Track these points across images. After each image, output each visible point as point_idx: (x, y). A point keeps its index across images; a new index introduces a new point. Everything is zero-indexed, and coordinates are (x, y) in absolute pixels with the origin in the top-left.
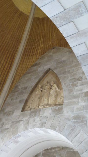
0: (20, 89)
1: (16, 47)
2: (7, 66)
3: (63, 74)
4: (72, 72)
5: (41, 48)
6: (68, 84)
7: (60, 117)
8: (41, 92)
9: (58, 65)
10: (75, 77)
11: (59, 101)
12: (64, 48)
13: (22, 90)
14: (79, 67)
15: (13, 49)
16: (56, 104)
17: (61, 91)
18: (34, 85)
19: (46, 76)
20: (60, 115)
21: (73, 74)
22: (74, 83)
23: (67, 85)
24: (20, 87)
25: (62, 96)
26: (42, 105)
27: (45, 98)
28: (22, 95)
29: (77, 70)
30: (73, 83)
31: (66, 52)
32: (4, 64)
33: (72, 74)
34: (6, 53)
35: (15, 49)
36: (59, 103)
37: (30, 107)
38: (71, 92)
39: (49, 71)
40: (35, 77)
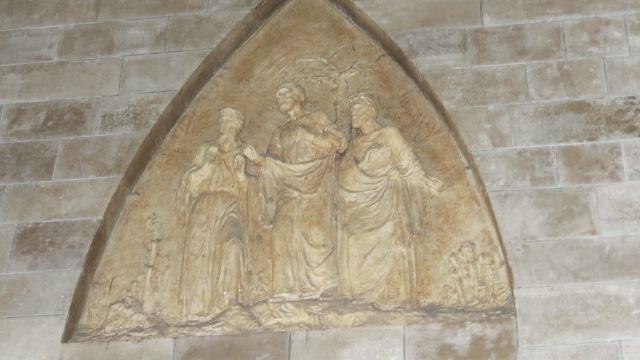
3: (463, 47)
4: (545, 54)
6: (525, 144)
8: (241, 176)
10: (582, 97)
14: (606, 15)
21: (560, 67)
22: (586, 143)
23: (520, 153)
27: (306, 236)
28: (43, 183)
29: (594, 43)
30: (574, 143)
33: (553, 61)
38: (570, 214)
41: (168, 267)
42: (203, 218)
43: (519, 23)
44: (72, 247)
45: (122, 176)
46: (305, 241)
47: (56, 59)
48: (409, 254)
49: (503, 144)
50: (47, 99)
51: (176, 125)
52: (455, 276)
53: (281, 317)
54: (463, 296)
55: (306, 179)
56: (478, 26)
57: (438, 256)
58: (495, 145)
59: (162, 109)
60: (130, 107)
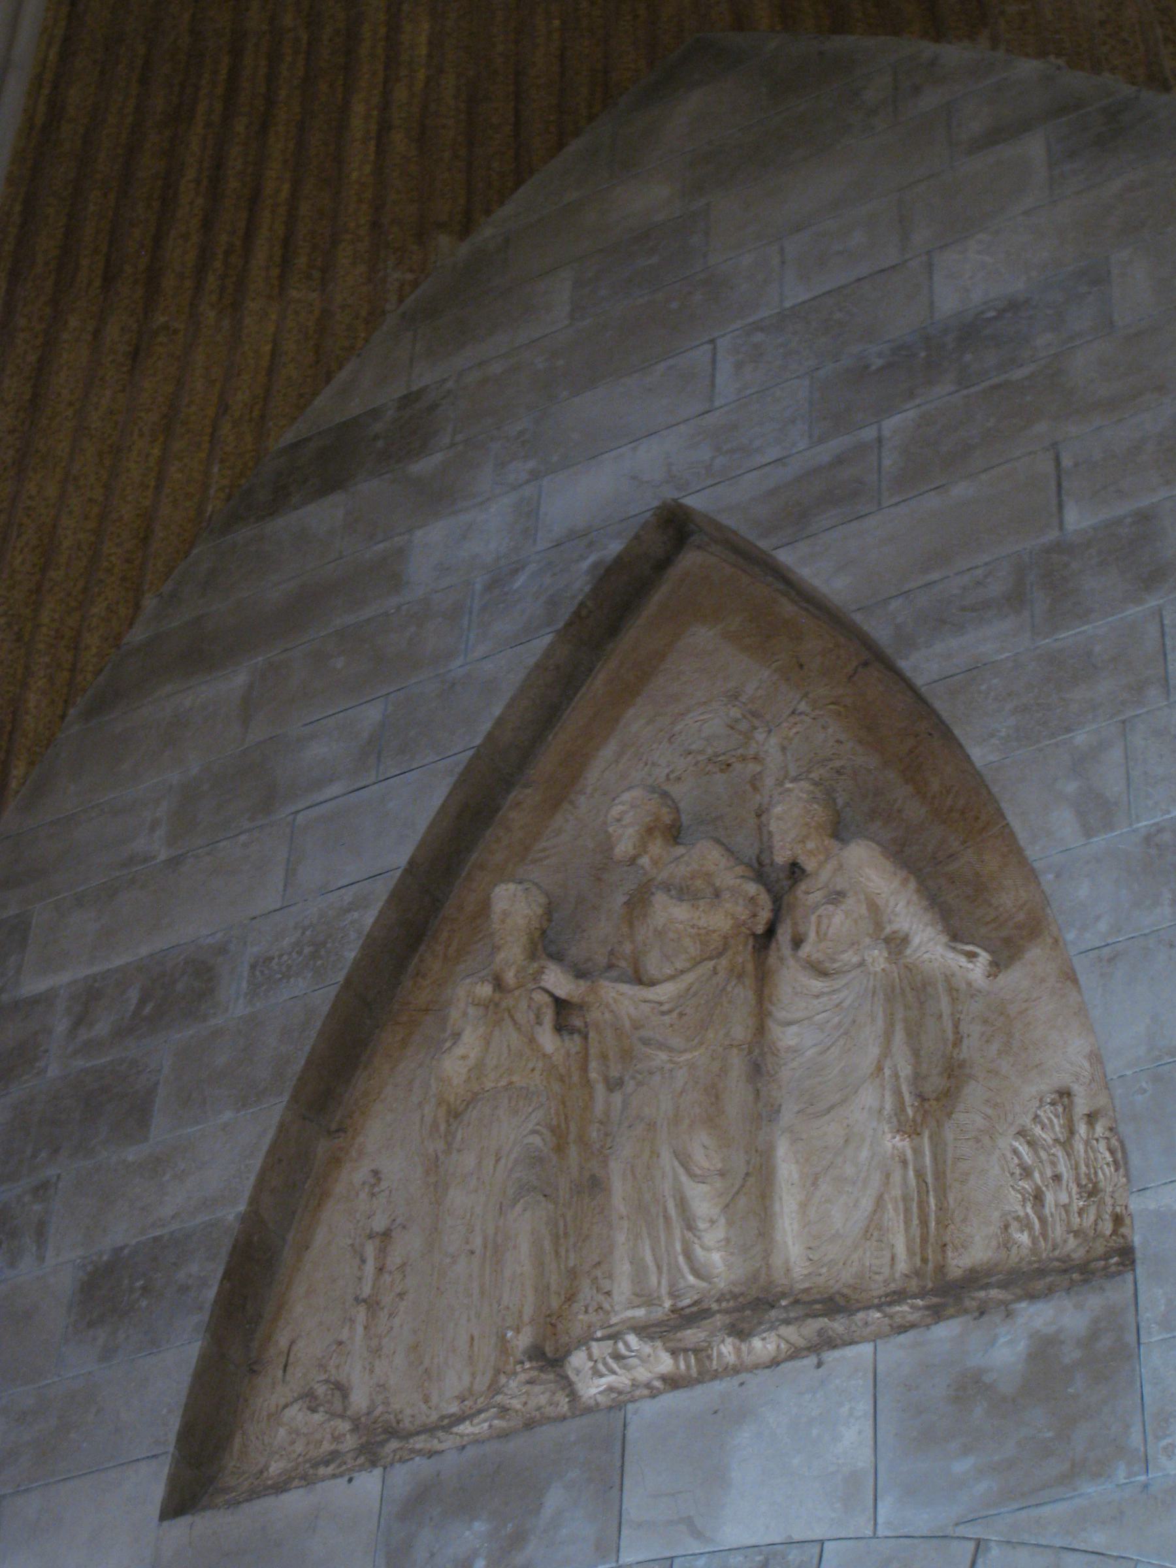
0: (61, 1026)
3: (1016, 599)
5: (400, 93)
7: (1098, 1539)
8: (548, 1040)
9: (869, 434)
11: (1014, 1203)
12: (929, 48)
13: (102, 1028)
16: (959, 1263)
17: (1014, 978)
18: (382, 890)
19: (598, 684)
20: (1091, 1489)
23: (1148, 839)
24: (33, 986)
25: (1062, 1079)
26: (644, 1330)
27: (684, 1159)
28: (132, 1154)
31: (996, 135)
36: (1007, 1244)
37: (359, 1400)
39: (663, 565)
40: (372, 714)
41: (401, 1295)
42: (469, 1161)
43: (1144, 502)
44: (184, 1289)
45: (286, 1097)
46: (681, 1171)
47: (163, 855)
48: (917, 1151)
49: (1109, 826)
50: (144, 951)
51: (423, 948)
52: (1025, 1184)
53: (614, 1372)
54: (1044, 1235)
55: (681, 1015)
56: (1053, 535)
57: (986, 1140)
58: (1088, 832)
59: (369, 918)
60: (305, 929)
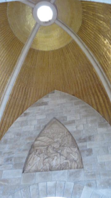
1: (93, 75)
2: (101, 100)
15: (93, 79)
32: (97, 101)
34: (90, 90)
35: (94, 77)
